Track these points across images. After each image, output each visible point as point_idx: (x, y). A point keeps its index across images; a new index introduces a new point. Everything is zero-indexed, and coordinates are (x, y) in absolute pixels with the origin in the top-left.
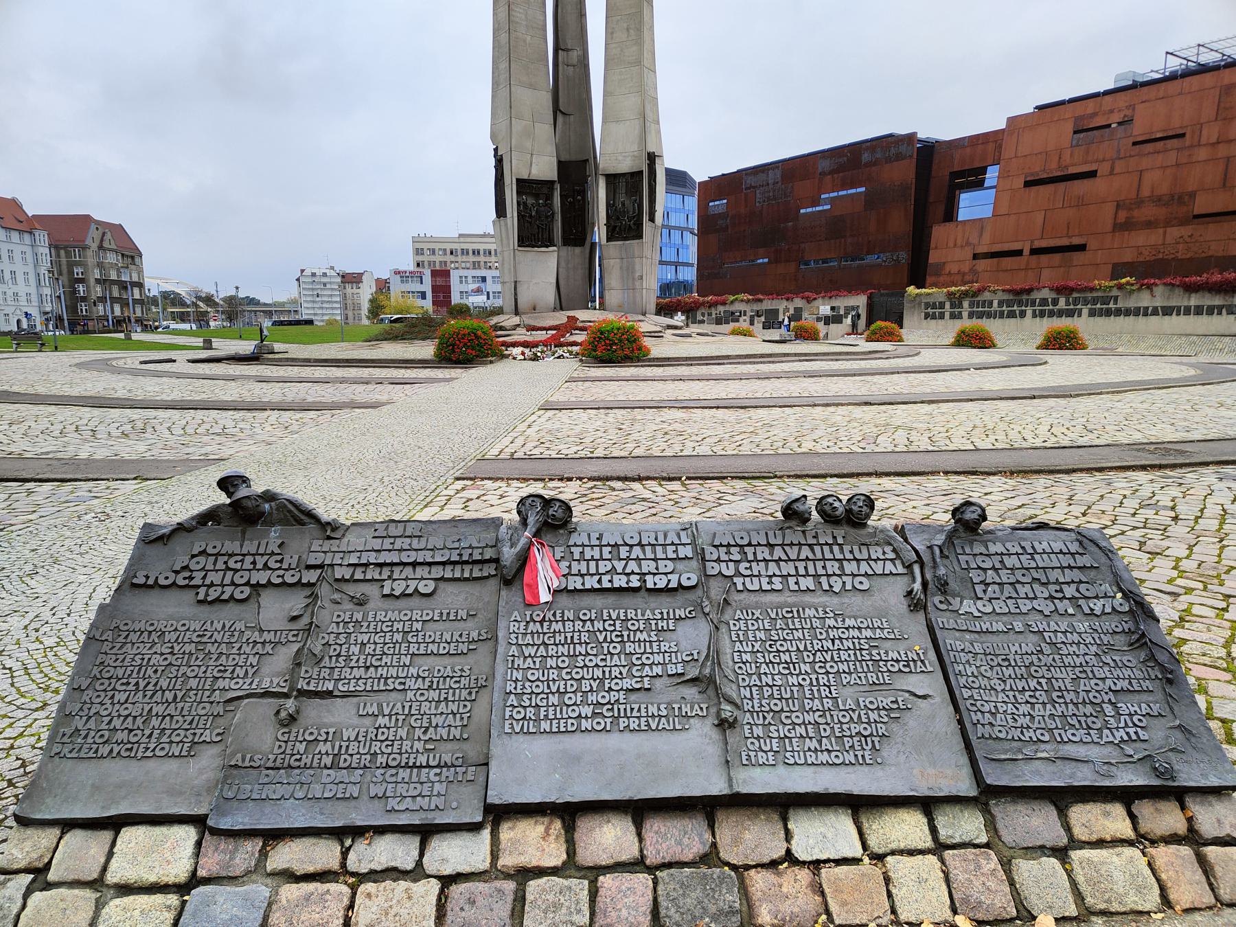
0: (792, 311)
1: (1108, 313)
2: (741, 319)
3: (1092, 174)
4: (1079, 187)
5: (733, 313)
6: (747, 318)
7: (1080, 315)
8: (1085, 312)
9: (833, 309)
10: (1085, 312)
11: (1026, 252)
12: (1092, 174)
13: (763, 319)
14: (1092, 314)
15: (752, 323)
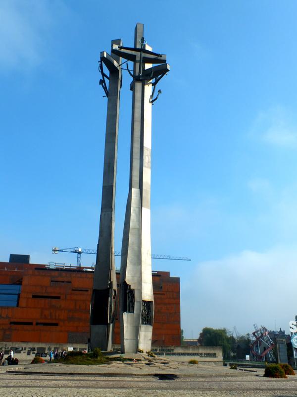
0: (53, 349)
1: (171, 354)
2: (22, 352)
3: (58, 298)
4: (54, 302)
5: (17, 349)
6: (26, 351)
7: (163, 355)
8: (165, 354)
9: (74, 349)
10: (165, 354)
11: (34, 323)
12: (58, 298)
13: (36, 352)
14: (167, 354)
15: (29, 354)
